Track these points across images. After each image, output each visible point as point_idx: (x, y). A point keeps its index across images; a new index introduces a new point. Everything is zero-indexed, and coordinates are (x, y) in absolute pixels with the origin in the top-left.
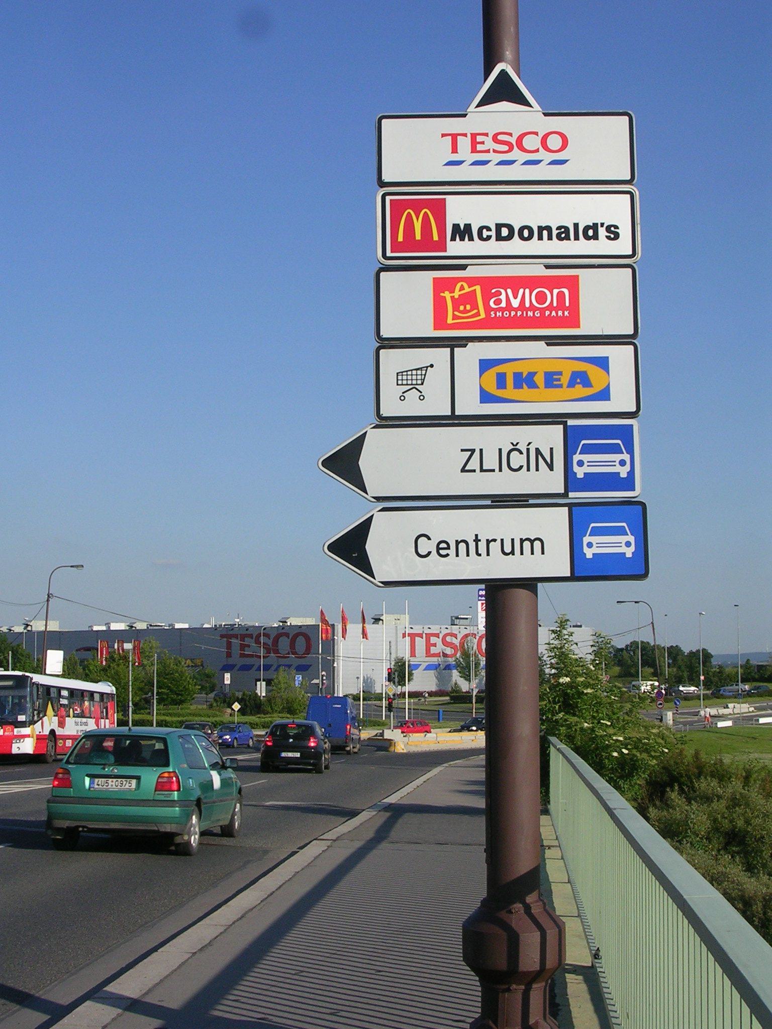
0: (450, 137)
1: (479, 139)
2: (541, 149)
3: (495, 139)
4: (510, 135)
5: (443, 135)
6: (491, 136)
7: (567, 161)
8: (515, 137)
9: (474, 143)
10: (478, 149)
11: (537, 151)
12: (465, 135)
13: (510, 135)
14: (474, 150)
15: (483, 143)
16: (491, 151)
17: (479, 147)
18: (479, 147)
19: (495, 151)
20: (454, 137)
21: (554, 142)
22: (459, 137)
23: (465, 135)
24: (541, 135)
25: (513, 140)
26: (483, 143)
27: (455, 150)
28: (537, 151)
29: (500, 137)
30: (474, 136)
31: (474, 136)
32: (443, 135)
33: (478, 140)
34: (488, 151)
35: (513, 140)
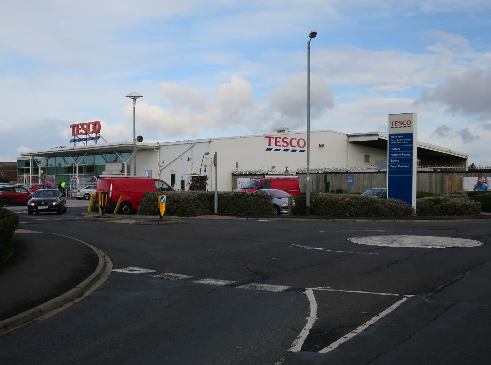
0: (268, 138)
1: (278, 140)
2: (297, 146)
6: (282, 139)
8: (289, 139)
9: (276, 142)
11: (296, 146)
14: (276, 145)
15: (279, 142)
16: (282, 145)
17: (278, 144)
18: (278, 144)
19: (283, 146)
20: (270, 138)
22: (271, 138)
23: (273, 138)
24: (297, 140)
26: (279, 142)
27: (270, 145)
30: (276, 138)
31: (276, 138)
34: (280, 146)
35: (288, 141)
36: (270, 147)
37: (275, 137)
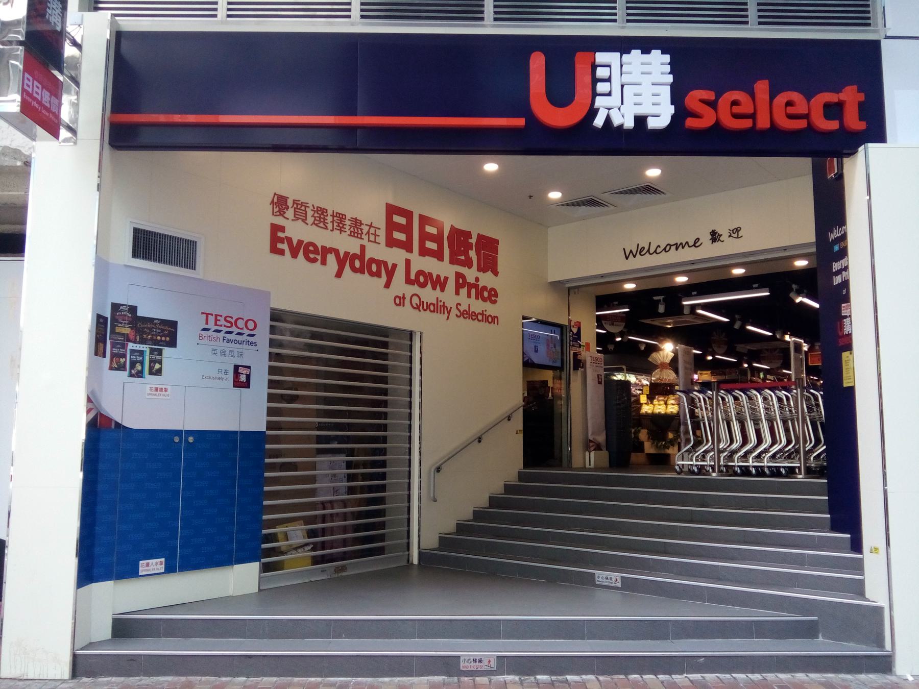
1: (219, 318)
2: (245, 328)
3: (226, 320)
4: (232, 318)
5: (203, 313)
6: (223, 317)
7: (255, 335)
8: (234, 318)
9: (216, 320)
10: (218, 324)
11: (242, 329)
12: (212, 315)
13: (232, 318)
14: (216, 324)
15: (219, 320)
18: (218, 323)
19: (225, 326)
20: (207, 315)
21: (251, 325)
22: (209, 316)
23: (212, 315)
25: (233, 321)
26: (219, 320)
27: (207, 323)
28: (242, 329)
29: (228, 319)
30: (216, 316)
32: (203, 313)
33: (218, 319)
34: (221, 326)
35: (233, 321)
36: (207, 327)
37: (215, 315)
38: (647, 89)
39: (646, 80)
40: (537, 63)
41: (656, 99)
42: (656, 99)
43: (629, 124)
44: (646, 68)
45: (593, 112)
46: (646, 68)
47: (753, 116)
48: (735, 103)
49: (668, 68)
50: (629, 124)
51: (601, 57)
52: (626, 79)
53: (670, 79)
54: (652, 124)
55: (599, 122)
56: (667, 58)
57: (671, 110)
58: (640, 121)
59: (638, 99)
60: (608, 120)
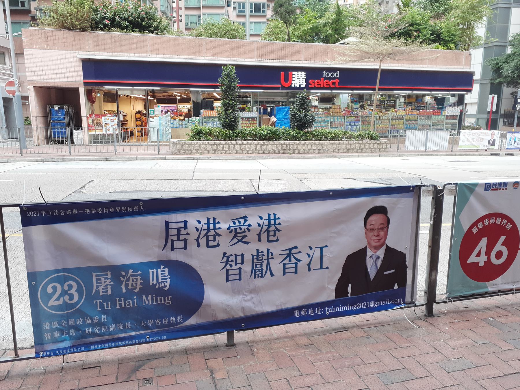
38: (301, 80)
39: (301, 78)
40: (282, 73)
41: (303, 82)
42: (303, 82)
43: (298, 86)
44: (301, 75)
45: (292, 84)
46: (301, 75)
47: (320, 85)
48: (318, 82)
49: (305, 75)
50: (298, 86)
51: (294, 73)
52: (298, 77)
53: (305, 78)
54: (302, 86)
55: (293, 86)
56: (305, 73)
57: (305, 84)
58: (300, 85)
59: (300, 82)
60: (294, 86)
